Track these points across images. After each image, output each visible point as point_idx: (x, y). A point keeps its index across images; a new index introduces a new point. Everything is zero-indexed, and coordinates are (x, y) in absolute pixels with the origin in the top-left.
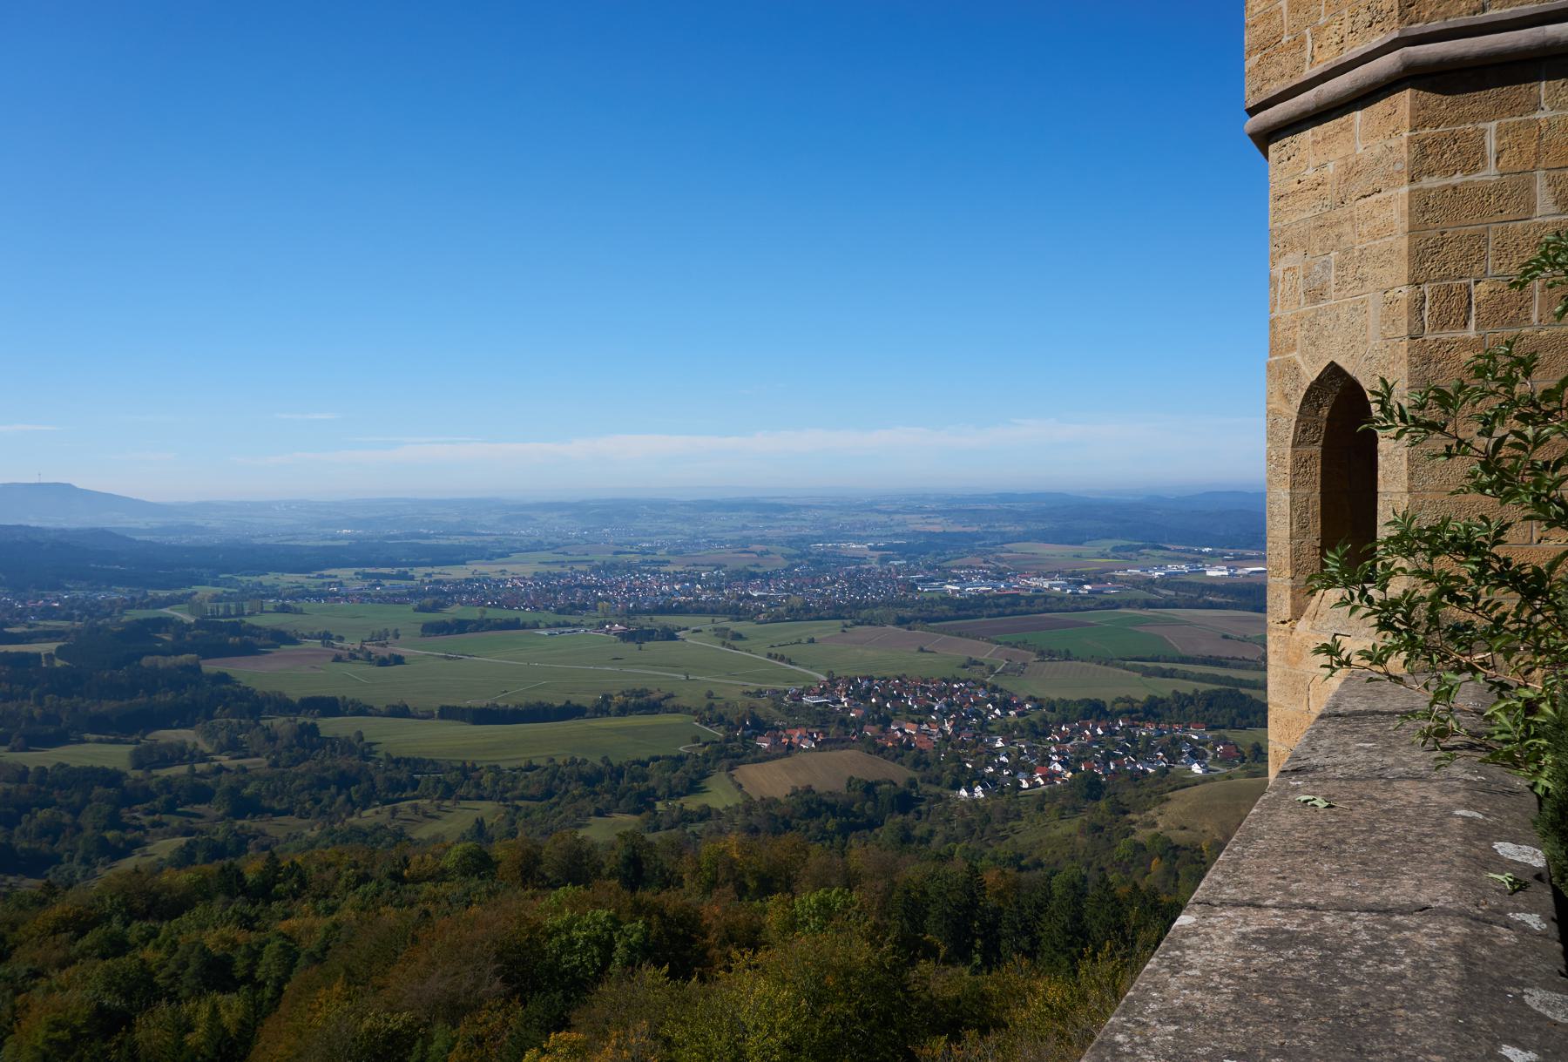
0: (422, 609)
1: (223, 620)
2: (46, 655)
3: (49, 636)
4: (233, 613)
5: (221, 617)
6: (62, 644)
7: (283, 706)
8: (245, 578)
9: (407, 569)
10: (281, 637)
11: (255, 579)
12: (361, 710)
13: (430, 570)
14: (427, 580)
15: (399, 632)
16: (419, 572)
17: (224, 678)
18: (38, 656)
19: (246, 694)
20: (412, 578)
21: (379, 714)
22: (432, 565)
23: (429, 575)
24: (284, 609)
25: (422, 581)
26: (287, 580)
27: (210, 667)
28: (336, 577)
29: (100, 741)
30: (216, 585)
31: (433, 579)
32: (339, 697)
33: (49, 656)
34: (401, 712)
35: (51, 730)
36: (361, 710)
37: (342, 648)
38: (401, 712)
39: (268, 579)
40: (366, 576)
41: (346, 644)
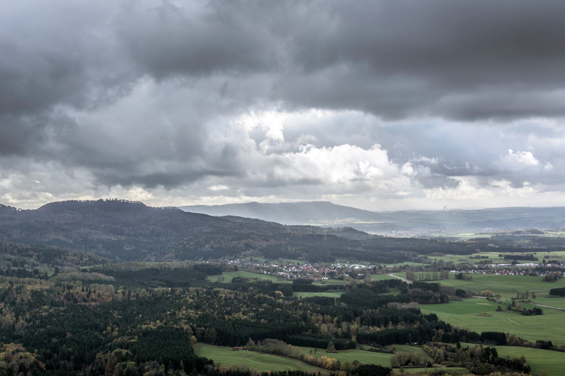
0: (547, 280)
1: (429, 282)
2: (336, 299)
3: (334, 288)
4: (431, 279)
5: (424, 281)
6: (344, 293)
7: (472, 337)
8: (433, 258)
9: (532, 253)
10: (461, 294)
11: (439, 258)
12: (520, 343)
13: (546, 253)
14: (547, 260)
15: (536, 294)
16: (540, 255)
17: (433, 317)
18: (332, 299)
19: (447, 327)
20: (536, 259)
21: (530, 346)
22: (549, 250)
23: (547, 257)
24: (459, 277)
25: (544, 261)
26: (456, 259)
27: (426, 310)
28: (487, 257)
29: (371, 350)
30: (416, 261)
31: (551, 260)
32: (506, 333)
33: (338, 299)
34: (546, 346)
35: (347, 342)
36: (520, 343)
37: (501, 303)
38: (546, 346)
39: (447, 258)
40: (507, 257)
41: (503, 299)
